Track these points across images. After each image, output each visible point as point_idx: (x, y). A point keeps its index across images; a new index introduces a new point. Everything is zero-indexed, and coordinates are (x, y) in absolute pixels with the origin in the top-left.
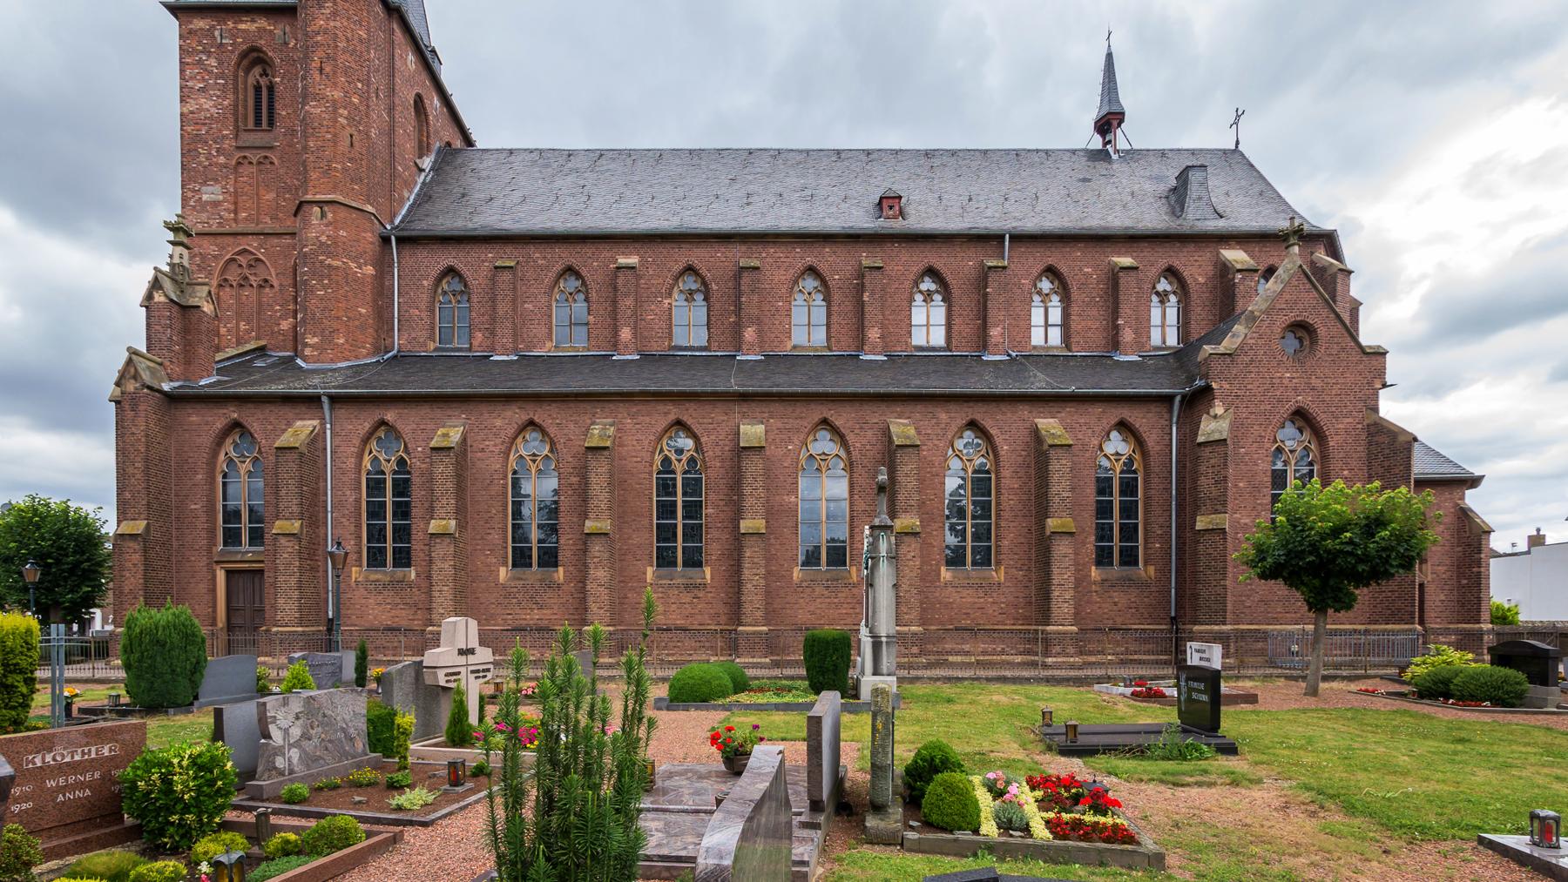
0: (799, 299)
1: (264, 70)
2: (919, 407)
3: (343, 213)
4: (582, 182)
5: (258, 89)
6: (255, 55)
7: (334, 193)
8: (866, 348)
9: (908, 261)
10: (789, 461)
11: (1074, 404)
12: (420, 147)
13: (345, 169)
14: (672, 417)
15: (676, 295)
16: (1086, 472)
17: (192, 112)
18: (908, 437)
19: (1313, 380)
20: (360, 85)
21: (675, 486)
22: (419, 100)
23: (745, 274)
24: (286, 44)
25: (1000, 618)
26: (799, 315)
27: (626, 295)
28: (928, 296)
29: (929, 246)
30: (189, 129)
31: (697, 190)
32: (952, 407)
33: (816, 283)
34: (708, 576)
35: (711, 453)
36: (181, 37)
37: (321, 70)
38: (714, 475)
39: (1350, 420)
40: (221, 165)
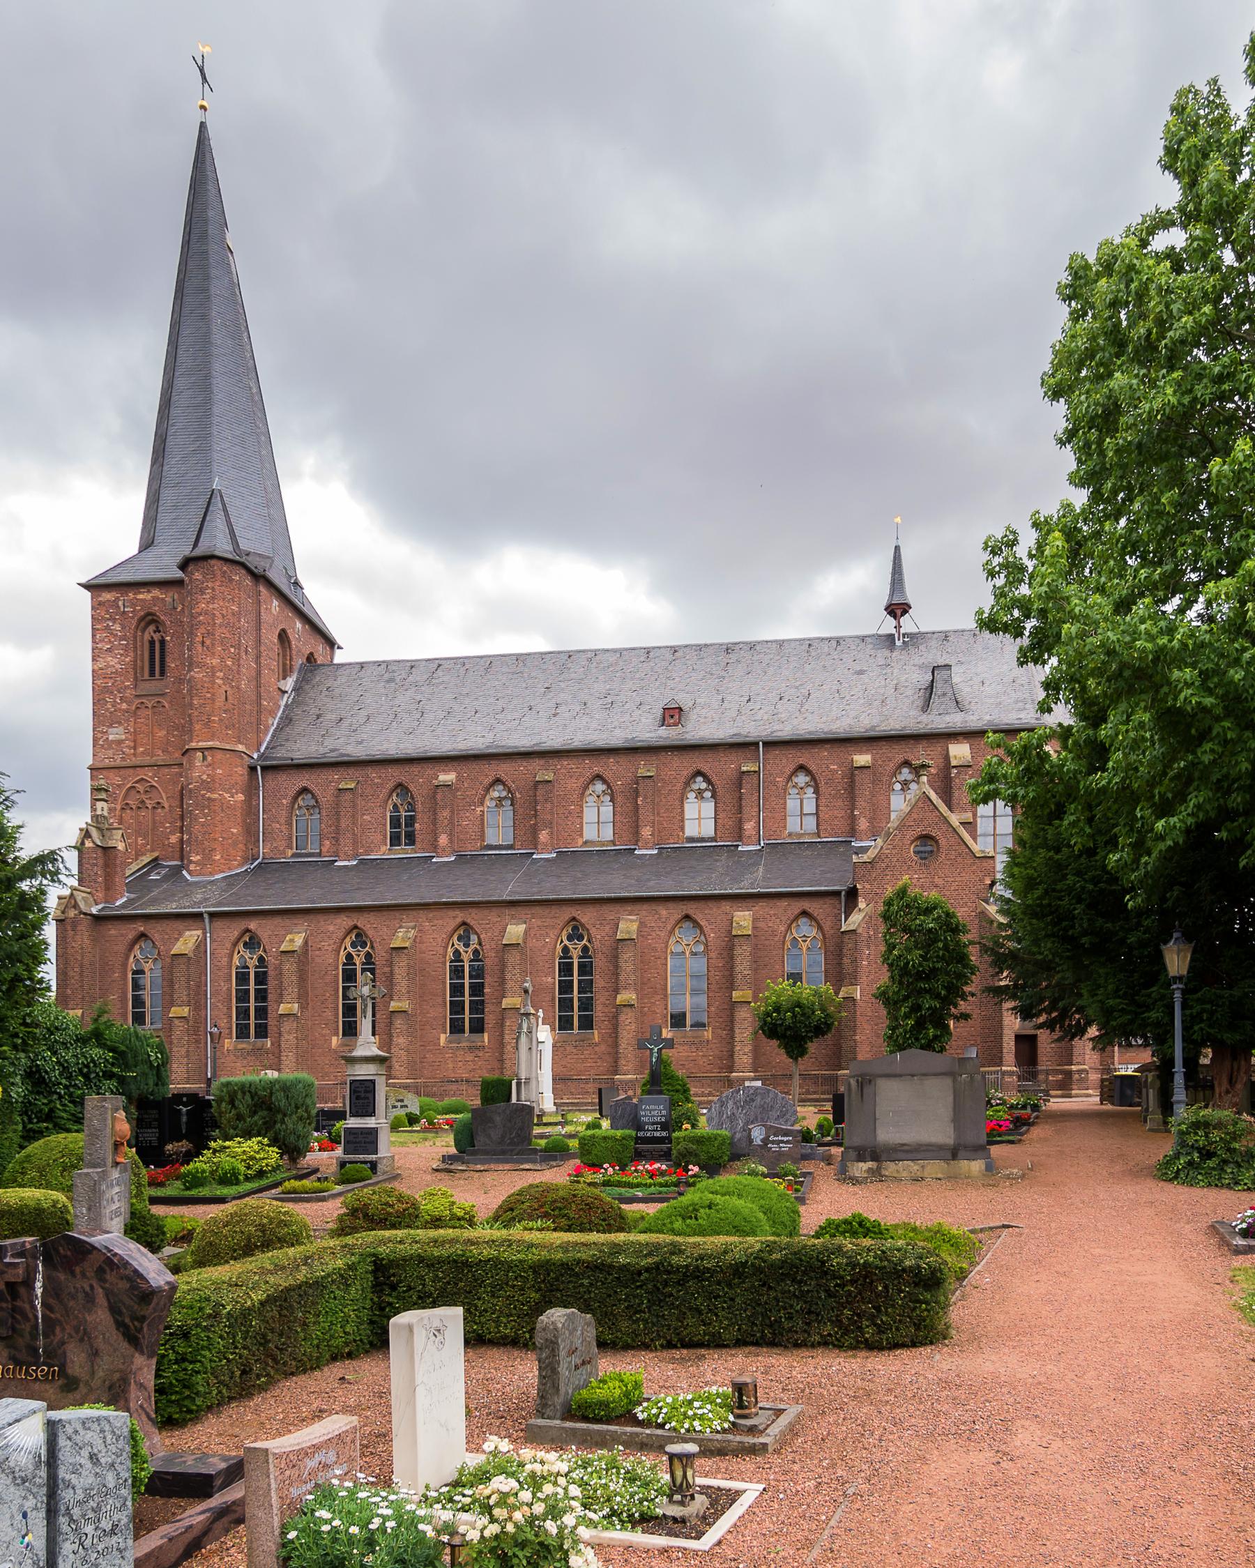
0: (591, 800)
1: (157, 627)
2: (646, 906)
3: (219, 755)
4: (418, 698)
5: (152, 643)
6: (150, 617)
7: (213, 740)
8: (640, 844)
9: (681, 766)
10: (546, 950)
11: (765, 900)
12: (284, 671)
13: (221, 720)
14: (459, 920)
15: (488, 803)
16: (775, 953)
17: (101, 669)
18: (628, 932)
19: (936, 879)
20: (232, 650)
21: (463, 971)
22: (283, 637)
23: (540, 786)
24: (175, 608)
25: (709, 1068)
26: (589, 814)
27: (444, 808)
28: (700, 793)
29: (697, 753)
30: (99, 682)
31: (515, 702)
32: (671, 905)
33: (604, 787)
34: (486, 1040)
35: (488, 947)
36: (93, 608)
37: (203, 642)
38: (490, 962)
39: (966, 909)
40: (124, 710)
